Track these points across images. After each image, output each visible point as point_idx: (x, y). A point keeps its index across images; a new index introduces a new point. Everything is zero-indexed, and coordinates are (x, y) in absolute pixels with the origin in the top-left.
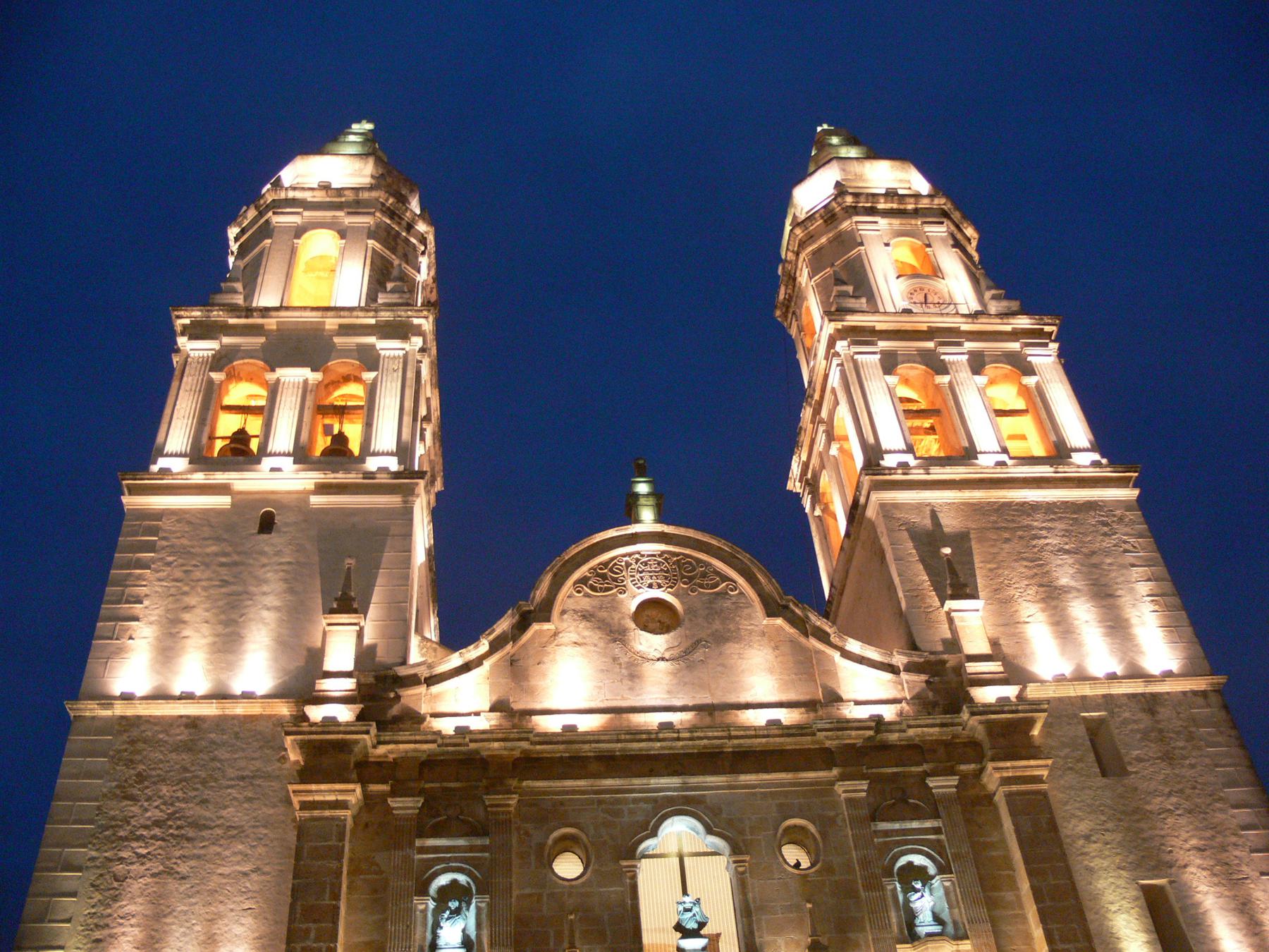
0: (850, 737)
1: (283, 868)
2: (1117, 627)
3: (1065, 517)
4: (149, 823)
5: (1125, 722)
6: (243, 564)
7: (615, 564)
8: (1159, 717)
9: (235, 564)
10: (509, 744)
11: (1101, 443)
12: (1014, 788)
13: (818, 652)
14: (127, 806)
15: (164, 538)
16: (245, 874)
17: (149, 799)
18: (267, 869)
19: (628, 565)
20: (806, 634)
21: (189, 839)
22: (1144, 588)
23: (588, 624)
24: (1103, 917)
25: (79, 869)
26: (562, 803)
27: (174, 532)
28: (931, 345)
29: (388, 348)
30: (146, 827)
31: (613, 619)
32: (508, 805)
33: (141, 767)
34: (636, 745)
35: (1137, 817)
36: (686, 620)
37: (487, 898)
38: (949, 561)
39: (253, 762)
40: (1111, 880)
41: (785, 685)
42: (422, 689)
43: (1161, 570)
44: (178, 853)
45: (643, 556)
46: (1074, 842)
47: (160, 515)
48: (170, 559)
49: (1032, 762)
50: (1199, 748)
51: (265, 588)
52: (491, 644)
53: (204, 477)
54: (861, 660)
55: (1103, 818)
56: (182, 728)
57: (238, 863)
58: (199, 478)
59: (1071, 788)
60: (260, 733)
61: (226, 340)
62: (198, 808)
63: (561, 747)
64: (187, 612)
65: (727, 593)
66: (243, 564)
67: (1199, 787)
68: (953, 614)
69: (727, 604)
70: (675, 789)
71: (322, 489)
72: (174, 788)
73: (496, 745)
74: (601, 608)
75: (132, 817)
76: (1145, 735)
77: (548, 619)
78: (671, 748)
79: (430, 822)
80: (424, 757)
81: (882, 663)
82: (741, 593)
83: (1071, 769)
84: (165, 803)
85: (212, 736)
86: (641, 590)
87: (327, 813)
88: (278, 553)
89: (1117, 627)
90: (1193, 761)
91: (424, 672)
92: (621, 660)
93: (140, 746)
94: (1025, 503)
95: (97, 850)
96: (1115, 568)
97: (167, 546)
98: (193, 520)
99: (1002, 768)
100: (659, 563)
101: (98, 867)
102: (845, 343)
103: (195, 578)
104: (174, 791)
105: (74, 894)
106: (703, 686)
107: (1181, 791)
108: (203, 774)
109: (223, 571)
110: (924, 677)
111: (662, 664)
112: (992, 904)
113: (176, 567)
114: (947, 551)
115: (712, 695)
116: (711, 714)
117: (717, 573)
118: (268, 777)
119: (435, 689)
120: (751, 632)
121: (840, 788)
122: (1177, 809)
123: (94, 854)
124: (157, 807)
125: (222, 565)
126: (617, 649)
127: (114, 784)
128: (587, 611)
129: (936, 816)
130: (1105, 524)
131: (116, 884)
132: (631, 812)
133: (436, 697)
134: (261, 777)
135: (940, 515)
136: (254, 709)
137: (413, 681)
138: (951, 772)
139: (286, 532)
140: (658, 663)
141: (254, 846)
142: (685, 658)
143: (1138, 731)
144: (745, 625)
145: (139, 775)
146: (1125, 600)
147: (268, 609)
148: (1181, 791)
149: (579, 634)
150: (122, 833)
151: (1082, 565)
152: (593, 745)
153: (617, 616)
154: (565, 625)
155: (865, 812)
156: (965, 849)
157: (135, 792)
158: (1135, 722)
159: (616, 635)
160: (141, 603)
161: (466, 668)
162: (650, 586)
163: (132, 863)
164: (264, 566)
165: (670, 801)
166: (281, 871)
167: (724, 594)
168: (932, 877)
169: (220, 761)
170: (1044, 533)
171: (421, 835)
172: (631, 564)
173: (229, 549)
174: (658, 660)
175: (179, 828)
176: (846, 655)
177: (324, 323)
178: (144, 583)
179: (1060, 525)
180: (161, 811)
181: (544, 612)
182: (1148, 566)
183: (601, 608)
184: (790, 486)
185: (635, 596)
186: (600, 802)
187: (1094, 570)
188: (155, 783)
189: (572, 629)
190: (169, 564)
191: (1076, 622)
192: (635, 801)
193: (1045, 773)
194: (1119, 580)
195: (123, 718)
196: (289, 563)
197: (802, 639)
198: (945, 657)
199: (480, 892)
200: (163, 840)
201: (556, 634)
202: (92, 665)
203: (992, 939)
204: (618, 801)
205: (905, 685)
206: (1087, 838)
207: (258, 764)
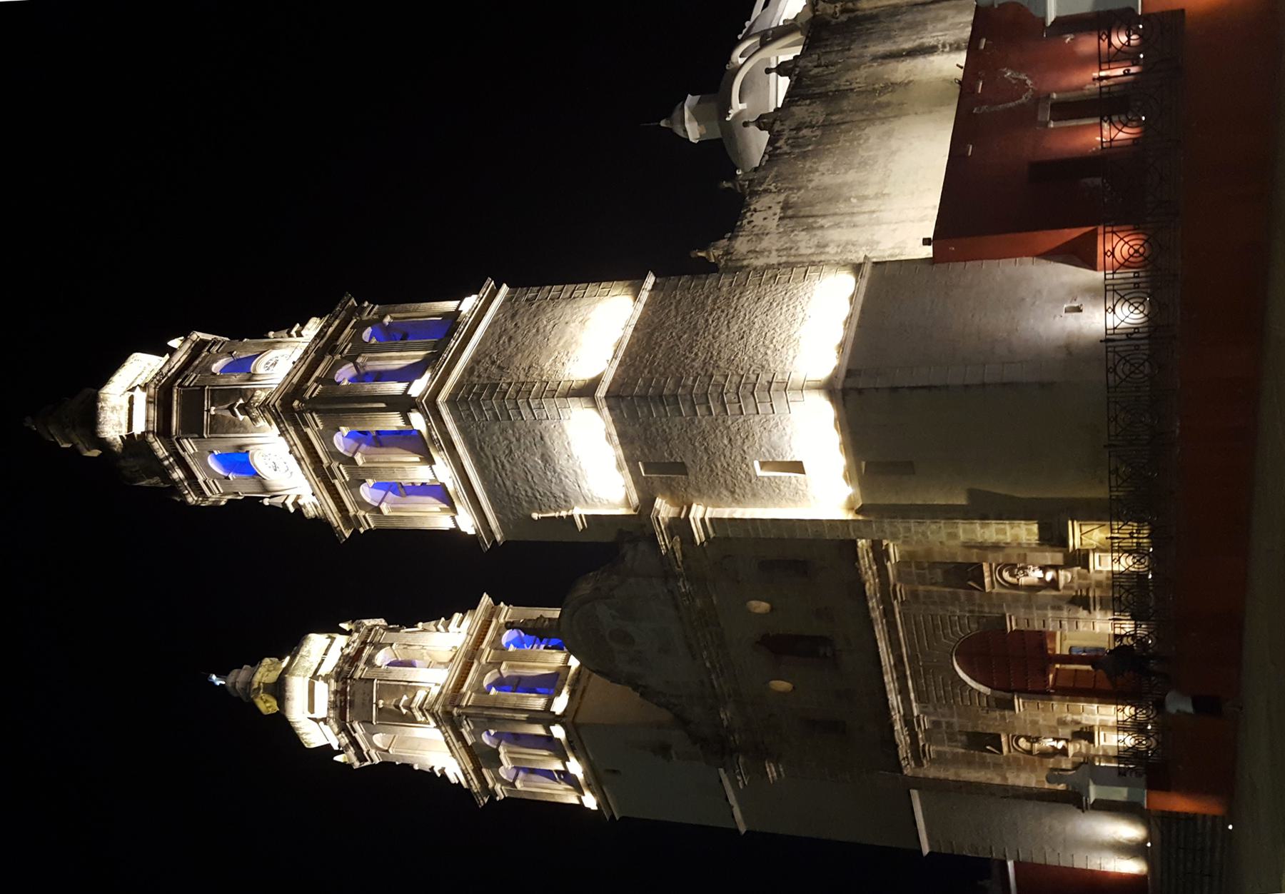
83: (685, 489)
122: (703, 445)
148: (690, 439)
158: (642, 450)
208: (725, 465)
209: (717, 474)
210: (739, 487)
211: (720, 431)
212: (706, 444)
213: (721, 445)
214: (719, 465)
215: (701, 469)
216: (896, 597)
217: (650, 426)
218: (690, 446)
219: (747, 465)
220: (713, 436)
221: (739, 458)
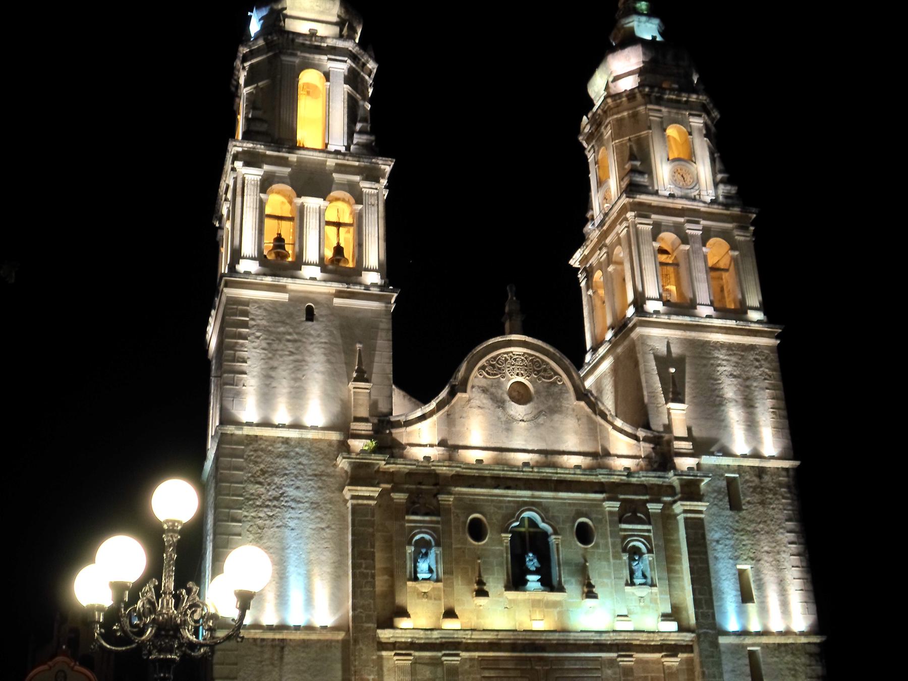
0: (614, 478)
1: (341, 527)
3: (737, 354)
4: (271, 498)
5: (747, 481)
6: (300, 341)
7: (499, 359)
8: (763, 480)
9: (295, 341)
10: (451, 468)
11: (765, 307)
12: (689, 515)
13: (601, 425)
14: (258, 488)
15: (253, 319)
16: (323, 529)
17: (269, 484)
18: (333, 527)
19: (506, 360)
20: (595, 414)
21: (292, 508)
22: (769, 403)
23: (486, 396)
24: (719, 580)
25: (240, 521)
26: (474, 500)
27: (257, 315)
28: (682, 220)
30: (270, 500)
31: (498, 393)
32: (449, 501)
33: (262, 466)
34: (511, 473)
35: (742, 533)
36: (535, 398)
37: (441, 549)
38: (673, 376)
39: (320, 466)
40: (724, 564)
41: (582, 442)
42: (403, 430)
43: (780, 393)
44: (289, 516)
45: (514, 355)
46: (711, 543)
47: (247, 303)
48: (258, 334)
49: (700, 503)
50: (778, 499)
51: (314, 358)
52: (437, 404)
53: (271, 280)
54: (621, 431)
55: (727, 532)
56: (280, 444)
57: (319, 523)
58: (268, 280)
59: (714, 515)
60: (321, 449)
61: (266, 167)
62: (295, 491)
63: (475, 471)
64: (273, 371)
65: (556, 383)
66: (300, 341)
67: (774, 520)
68: (671, 411)
69: (556, 390)
70: (528, 497)
71: (340, 294)
72: (281, 479)
73: (445, 468)
74: (492, 386)
75: (262, 494)
76: (755, 488)
77: (465, 391)
78: (528, 475)
79: (412, 507)
80: (407, 471)
81: (631, 434)
82: (563, 384)
83: (715, 504)
84: (277, 487)
85: (297, 450)
86: (513, 377)
87: (365, 502)
88: (319, 336)
90: (775, 506)
91: (403, 419)
92: (502, 420)
93: (260, 453)
94: (718, 342)
95: (247, 512)
96: (757, 389)
97: (255, 325)
98: (267, 307)
99: (685, 505)
100: (522, 360)
101: (249, 521)
102: (633, 214)
103: (273, 348)
104: (281, 481)
105: (240, 535)
106: (543, 439)
107: (765, 522)
108: (295, 472)
109: (290, 345)
110: (652, 446)
111: (522, 424)
112: (670, 570)
113: (263, 340)
114: (672, 370)
115: (547, 444)
116: (546, 457)
117: (552, 369)
118: (329, 475)
119: (409, 429)
120: (568, 408)
121: (607, 504)
123: (246, 514)
124: (274, 489)
125: (289, 341)
126: (499, 412)
127: (250, 475)
128: (485, 387)
129: (649, 523)
130: (757, 360)
131: (259, 531)
132: (507, 507)
133: (409, 434)
134: (325, 475)
135: (672, 346)
137: (398, 424)
138: (658, 501)
139: (322, 321)
140: (521, 422)
141: (325, 514)
143: (751, 487)
144: (565, 404)
145: (261, 470)
147: (317, 372)
148: (765, 522)
149: (481, 401)
150: (258, 503)
151: (741, 385)
152: (491, 472)
153: (500, 392)
154: (474, 395)
155: (616, 518)
156: (661, 543)
157: (261, 480)
159: (500, 404)
160: (246, 362)
161: (423, 418)
162: (518, 375)
163: (266, 520)
164: (312, 343)
165: (525, 503)
166: (340, 528)
167: (554, 384)
168: (644, 554)
169: (303, 464)
170: (724, 363)
171: (408, 513)
172: (508, 360)
173: (291, 330)
174: (521, 421)
175: (286, 502)
176: (615, 428)
177: (326, 161)
178: (246, 349)
179: (734, 359)
180: (276, 491)
181: (463, 387)
182: (774, 390)
183: (492, 386)
184: (571, 262)
186: (492, 501)
187: (746, 389)
188: (271, 476)
189: (477, 398)
190: (258, 338)
191: (732, 421)
192: (509, 502)
193: (704, 509)
194: (758, 397)
195: (247, 436)
196: (325, 343)
197: (593, 416)
198: (663, 435)
199: (438, 544)
200: (279, 508)
201: (469, 400)
203: (668, 588)
204: (501, 501)
205: (642, 449)
206: (718, 542)
207: (322, 468)
208: (744, 543)
209: (734, 534)
210: (723, 549)
211: (775, 547)
212: (762, 532)
213: (762, 544)
214: (743, 537)
215: (737, 522)
216: (619, 656)
217: (775, 494)
218: (759, 520)
219: (746, 560)
220: (771, 540)
221: (752, 555)
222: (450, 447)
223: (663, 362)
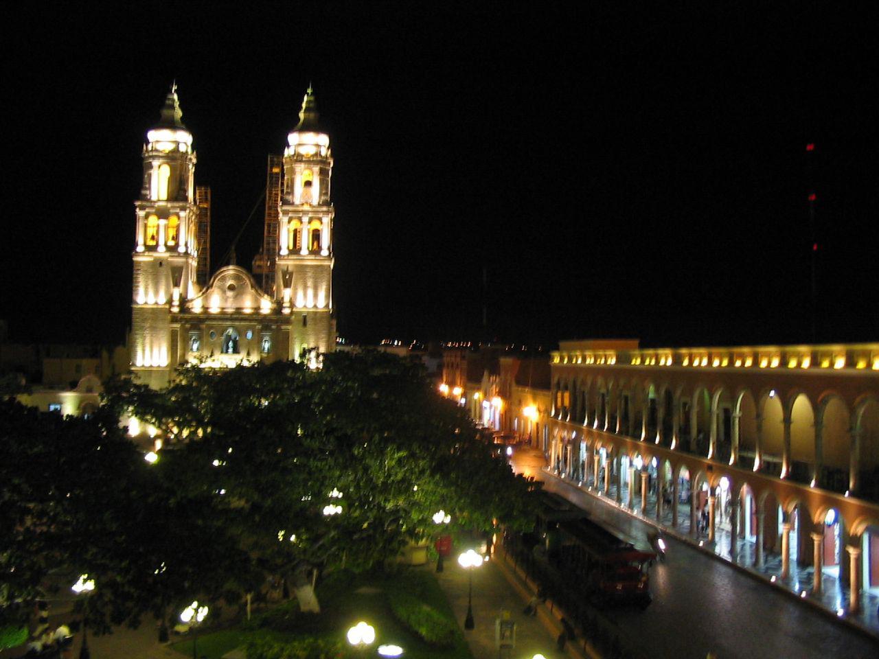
2: (316, 296)
29: (182, 214)
47: (140, 262)
71: (170, 256)
79: (191, 329)
89: (316, 296)
136: (162, 307)
142: (236, 297)
146: (319, 289)
159: (224, 292)
185: (230, 282)
202: (134, 297)
222: (205, 309)
223: (285, 273)
